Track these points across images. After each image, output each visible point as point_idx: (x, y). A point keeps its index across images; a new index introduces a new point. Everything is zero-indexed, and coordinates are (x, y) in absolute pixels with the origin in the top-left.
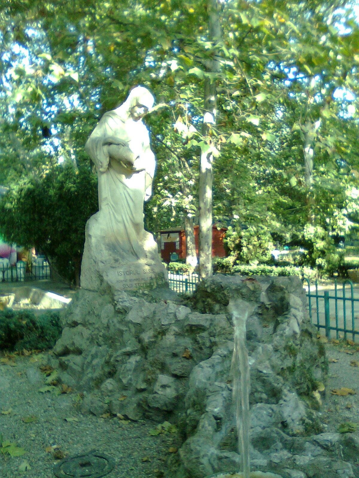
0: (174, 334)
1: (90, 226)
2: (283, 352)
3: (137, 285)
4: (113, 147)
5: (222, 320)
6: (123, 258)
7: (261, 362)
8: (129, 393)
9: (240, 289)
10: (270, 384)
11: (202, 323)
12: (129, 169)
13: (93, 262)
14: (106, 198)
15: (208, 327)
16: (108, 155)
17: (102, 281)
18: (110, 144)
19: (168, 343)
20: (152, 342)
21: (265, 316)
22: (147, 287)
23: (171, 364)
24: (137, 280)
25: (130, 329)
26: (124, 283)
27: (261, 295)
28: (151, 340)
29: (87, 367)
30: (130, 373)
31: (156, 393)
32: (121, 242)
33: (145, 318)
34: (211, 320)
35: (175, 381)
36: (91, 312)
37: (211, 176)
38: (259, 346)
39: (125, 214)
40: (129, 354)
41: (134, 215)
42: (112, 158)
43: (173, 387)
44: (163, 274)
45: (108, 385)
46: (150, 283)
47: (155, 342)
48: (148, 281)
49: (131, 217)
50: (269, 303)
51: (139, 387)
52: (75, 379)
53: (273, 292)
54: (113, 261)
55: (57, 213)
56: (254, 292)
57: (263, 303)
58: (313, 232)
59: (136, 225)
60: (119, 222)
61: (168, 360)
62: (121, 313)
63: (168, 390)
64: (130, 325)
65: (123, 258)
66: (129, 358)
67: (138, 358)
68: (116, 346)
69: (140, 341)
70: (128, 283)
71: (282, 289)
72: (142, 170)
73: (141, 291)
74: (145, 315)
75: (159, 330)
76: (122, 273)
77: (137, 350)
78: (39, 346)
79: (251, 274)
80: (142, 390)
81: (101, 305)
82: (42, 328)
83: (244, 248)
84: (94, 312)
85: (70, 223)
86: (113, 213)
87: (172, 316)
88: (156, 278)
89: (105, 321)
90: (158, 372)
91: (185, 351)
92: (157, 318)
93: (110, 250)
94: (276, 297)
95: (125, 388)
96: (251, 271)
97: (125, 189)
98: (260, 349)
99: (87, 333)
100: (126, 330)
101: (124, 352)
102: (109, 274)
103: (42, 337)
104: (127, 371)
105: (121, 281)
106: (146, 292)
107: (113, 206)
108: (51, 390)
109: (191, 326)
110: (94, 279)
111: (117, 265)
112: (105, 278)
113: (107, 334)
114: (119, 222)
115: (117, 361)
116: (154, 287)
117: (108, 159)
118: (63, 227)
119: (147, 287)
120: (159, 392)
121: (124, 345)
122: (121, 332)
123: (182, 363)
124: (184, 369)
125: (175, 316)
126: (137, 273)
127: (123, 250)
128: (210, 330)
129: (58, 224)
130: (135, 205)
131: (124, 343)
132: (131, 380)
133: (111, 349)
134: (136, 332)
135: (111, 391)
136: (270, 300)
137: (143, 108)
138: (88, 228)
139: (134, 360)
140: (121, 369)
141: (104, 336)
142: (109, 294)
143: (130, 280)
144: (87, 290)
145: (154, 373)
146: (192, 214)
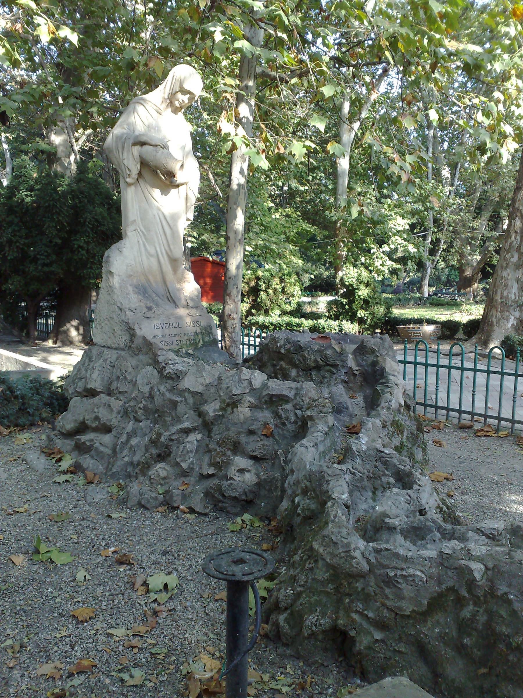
0: (249, 407)
1: (111, 259)
2: (390, 429)
5: (312, 390)
6: (157, 305)
7: (373, 441)
8: (192, 479)
10: (395, 465)
11: (285, 393)
12: (167, 182)
13: (117, 309)
14: (135, 220)
15: (293, 397)
16: (138, 160)
17: (133, 335)
18: (143, 144)
19: (242, 417)
20: (219, 416)
21: (350, 385)
22: (191, 344)
23: (247, 443)
25: (186, 400)
26: (162, 339)
27: (349, 359)
29: (122, 449)
30: (192, 455)
31: (231, 479)
32: (154, 284)
33: (208, 386)
34: (297, 389)
35: (254, 464)
36: (121, 377)
37: (245, 193)
38: (368, 421)
39: (159, 244)
40: (187, 432)
41: (172, 247)
42: (144, 163)
43: (253, 471)
45: (160, 470)
46: (195, 340)
47: (223, 416)
48: (192, 338)
50: (357, 368)
51: (205, 473)
52: (102, 465)
53: (363, 354)
54: (145, 310)
56: (341, 354)
57: (350, 368)
58: (356, 275)
59: (174, 261)
60: (152, 256)
61: (243, 439)
62: (172, 379)
63: (247, 476)
64: (186, 394)
65: (157, 305)
66: (188, 436)
67: (199, 436)
68: (165, 421)
69: (200, 414)
70: (168, 339)
71: (373, 351)
72: (182, 184)
73: (184, 351)
74: (208, 381)
75: (228, 401)
78: (20, 421)
79: (273, 327)
80: (209, 476)
81: (135, 368)
82: (23, 397)
83: (262, 293)
84: (125, 378)
87: (246, 383)
89: (146, 389)
90: (229, 453)
91: (265, 427)
92: (224, 386)
93: (139, 293)
94: (366, 361)
95: (184, 474)
96: (272, 324)
98: (370, 425)
99: (116, 404)
100: (181, 401)
101: (181, 429)
102: (142, 327)
103: (23, 410)
104: (188, 452)
106: (190, 352)
107: (142, 232)
108: (70, 480)
109: (271, 396)
110: (119, 332)
111: (149, 314)
112: (138, 332)
113: (150, 406)
114: (152, 256)
115: (172, 440)
116: (200, 345)
117: (139, 166)
119: (191, 344)
120: (235, 478)
121: (178, 420)
122: (175, 404)
123: (262, 443)
124: (265, 449)
125: (250, 383)
126: (179, 326)
128: (295, 402)
131: (178, 417)
132: (192, 463)
133: (157, 426)
134: (194, 403)
135: (164, 478)
136: (358, 365)
137: (188, 96)
138: (107, 262)
139: (194, 438)
140: (177, 450)
141: (145, 408)
142: (147, 354)
143: (170, 336)
144: (104, 347)
145: (224, 455)
146: (192, 242)
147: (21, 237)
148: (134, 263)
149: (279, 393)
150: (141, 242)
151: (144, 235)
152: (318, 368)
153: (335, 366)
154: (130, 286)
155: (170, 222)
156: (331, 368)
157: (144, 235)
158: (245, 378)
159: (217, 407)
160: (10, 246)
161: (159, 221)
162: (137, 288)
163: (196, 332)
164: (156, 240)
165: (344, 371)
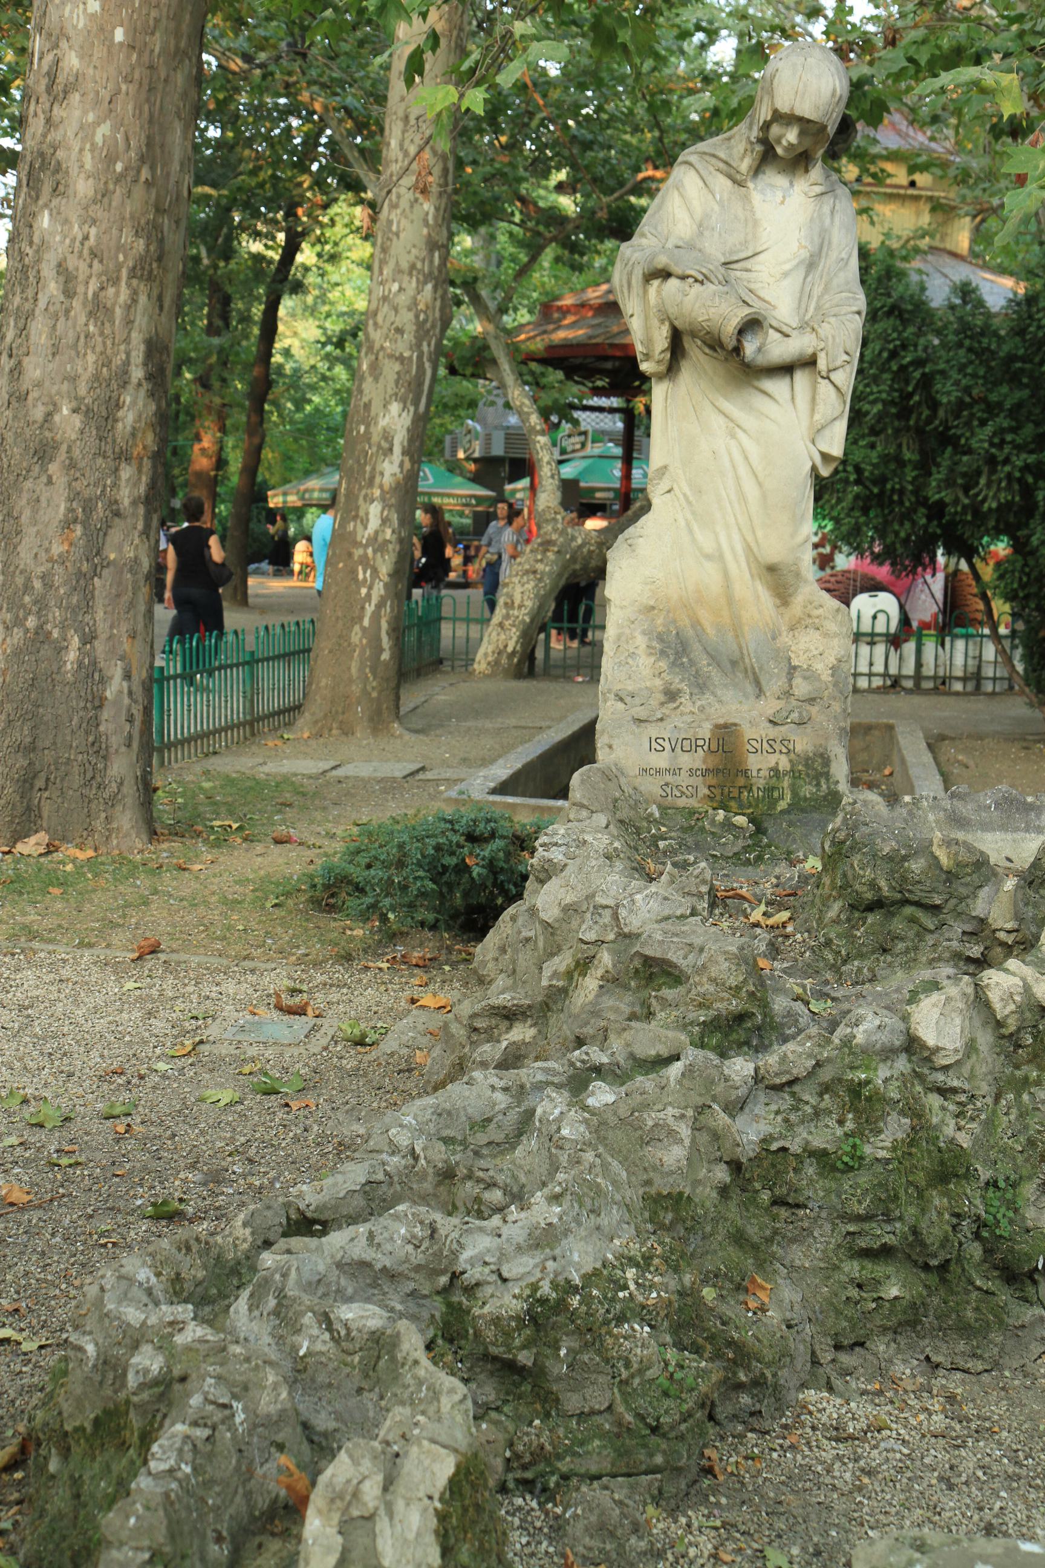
3: (717, 791)
4: (673, 282)
5: (721, 959)
9: (905, 858)
11: (675, 956)
14: (665, 467)
18: (665, 274)
26: (669, 778)
28: (554, 982)
32: (711, 631)
41: (760, 534)
44: (827, 762)
55: (981, 438)
56: (951, 876)
57: (982, 921)
60: (708, 557)
66: (510, 1028)
76: (666, 745)
77: (529, 1006)
85: (1030, 480)
86: (688, 524)
87: (607, 917)
88: (794, 774)
93: (663, 653)
97: (733, 436)
101: (493, 1008)
105: (658, 771)
107: (685, 495)
109: (648, 961)
116: (782, 805)
118: (1003, 497)
125: (616, 917)
127: (714, 658)
129: (983, 481)
130: (764, 497)
147: (1019, 448)
149: (658, 955)
150: (683, 523)
152: (877, 905)
153: (935, 909)
154: (644, 633)
156: (920, 914)
158: (604, 902)
159: (562, 968)
160: (993, 471)
161: (728, 464)
165: (958, 927)
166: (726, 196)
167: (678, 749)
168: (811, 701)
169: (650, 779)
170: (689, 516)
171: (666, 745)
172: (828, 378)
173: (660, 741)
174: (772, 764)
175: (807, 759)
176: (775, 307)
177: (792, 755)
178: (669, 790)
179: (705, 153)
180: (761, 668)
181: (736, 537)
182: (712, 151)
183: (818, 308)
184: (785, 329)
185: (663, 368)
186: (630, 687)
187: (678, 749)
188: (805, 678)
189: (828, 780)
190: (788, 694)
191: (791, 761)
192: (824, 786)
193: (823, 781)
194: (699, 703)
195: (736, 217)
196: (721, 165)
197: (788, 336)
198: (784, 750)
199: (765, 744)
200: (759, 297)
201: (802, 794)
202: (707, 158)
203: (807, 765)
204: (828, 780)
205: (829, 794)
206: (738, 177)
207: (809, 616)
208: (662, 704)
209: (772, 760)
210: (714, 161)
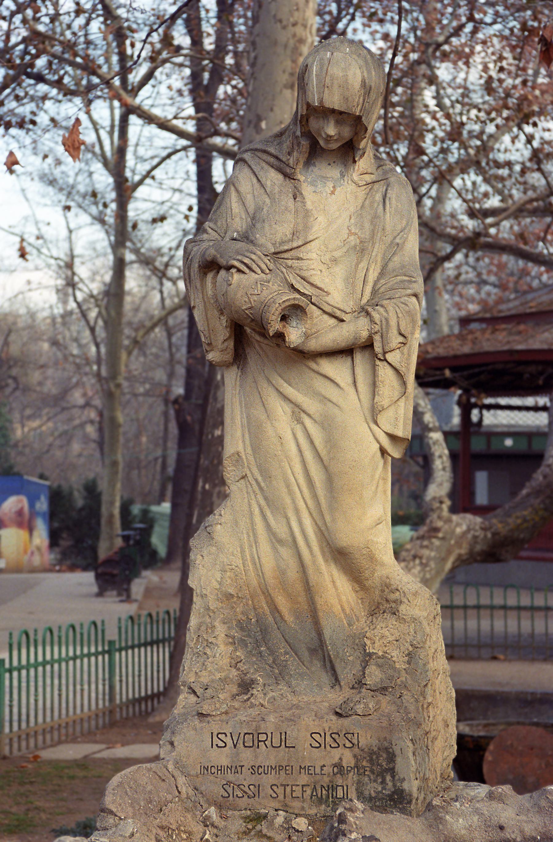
3: (280, 791)
24: (280, 768)
26: (231, 777)
41: (328, 518)
44: (392, 758)
48: (326, 780)
49: (320, 523)
76: (228, 740)
97: (299, 421)
105: (220, 769)
107: (256, 480)
114: (280, 541)
143: (255, 770)
148: (240, 562)
151: (261, 488)
155: (323, 453)
157: (261, 488)
162: (242, 629)
163: (338, 766)
164: (288, 500)
166: (277, 189)
167: (240, 745)
168: (383, 690)
169: (212, 778)
170: (262, 502)
171: (228, 740)
172: (385, 360)
173: (221, 736)
174: (336, 760)
175: (371, 753)
176: (328, 294)
177: (356, 750)
178: (230, 790)
179: (256, 150)
180: (337, 656)
181: (307, 522)
182: (264, 148)
183: (374, 292)
184: (338, 313)
185: (228, 357)
186: (205, 678)
187: (240, 745)
188: (379, 666)
189: (393, 777)
190: (359, 684)
191: (355, 756)
192: (390, 784)
193: (388, 778)
194: (271, 694)
195: (286, 209)
196: (272, 160)
197: (343, 321)
198: (348, 745)
199: (328, 738)
200: (312, 285)
201: (367, 793)
202: (259, 154)
203: (371, 761)
204: (393, 777)
205: (394, 793)
206: (288, 170)
207: (387, 601)
208: (234, 697)
209: (336, 755)
210: (265, 156)
